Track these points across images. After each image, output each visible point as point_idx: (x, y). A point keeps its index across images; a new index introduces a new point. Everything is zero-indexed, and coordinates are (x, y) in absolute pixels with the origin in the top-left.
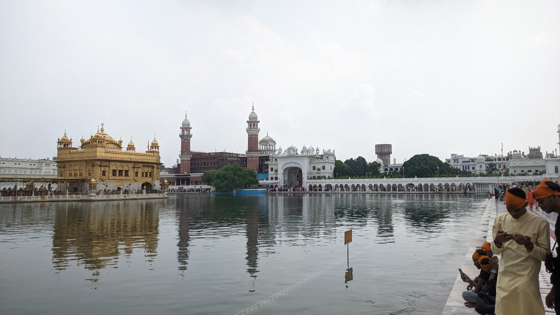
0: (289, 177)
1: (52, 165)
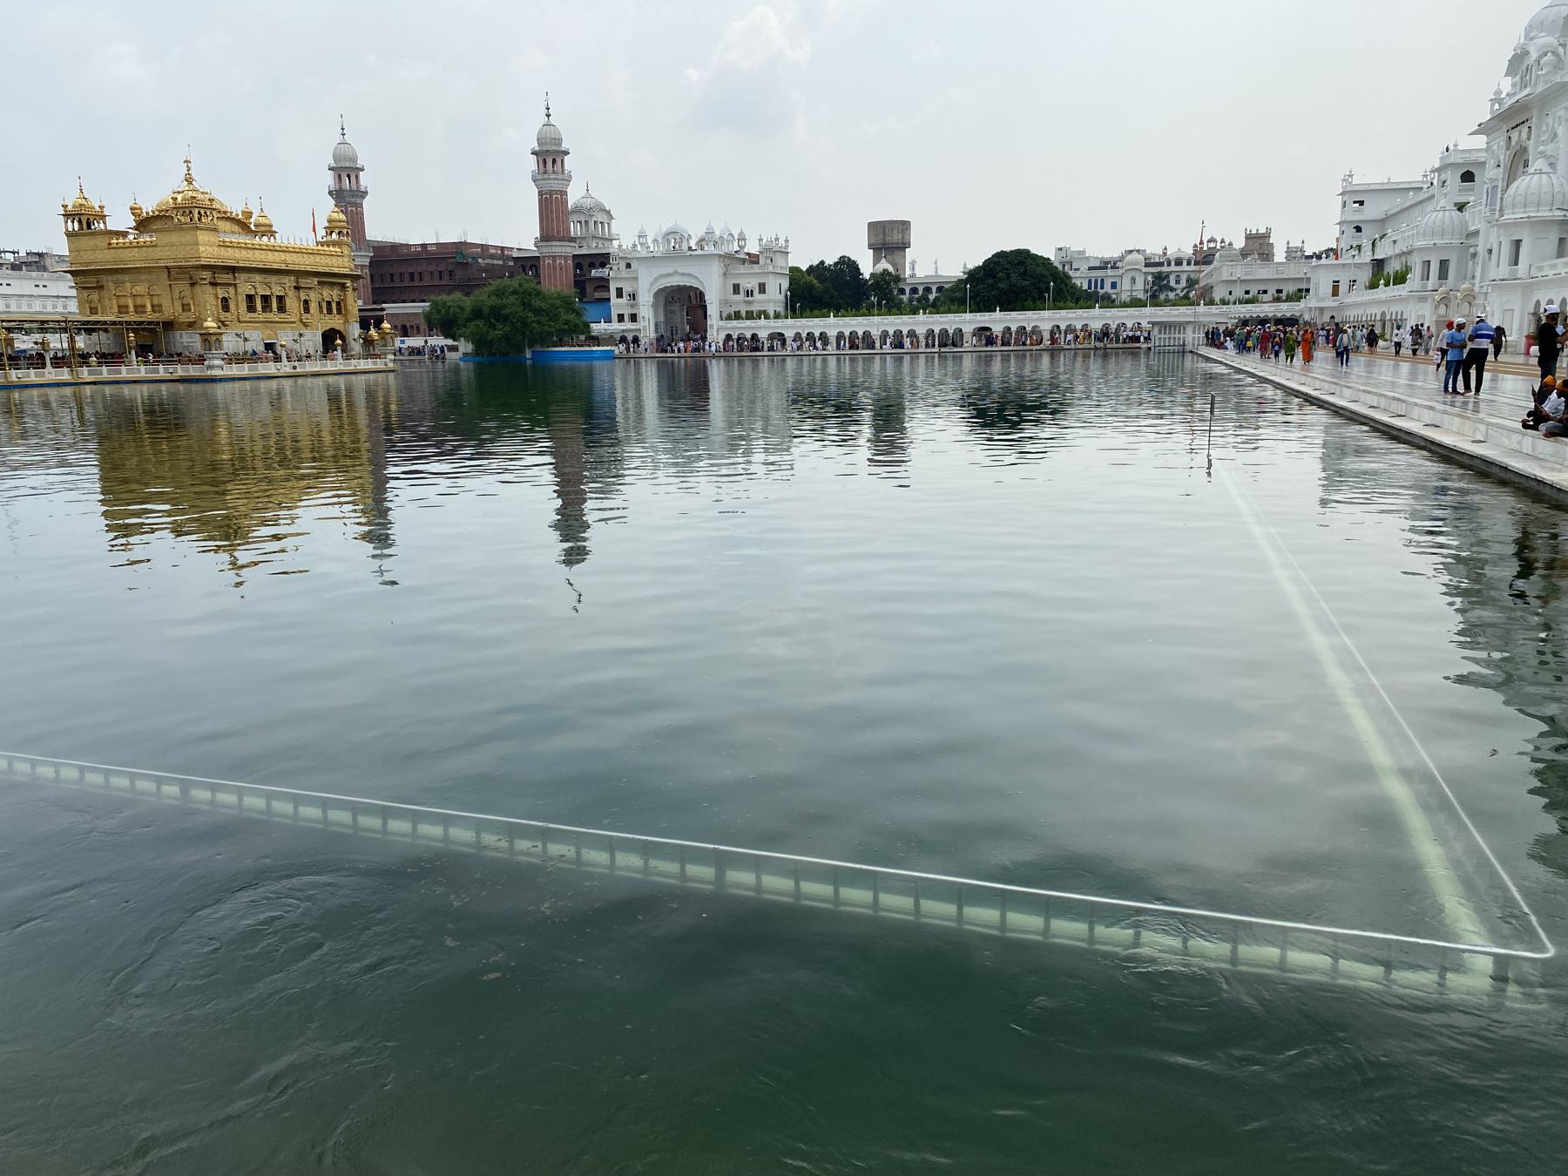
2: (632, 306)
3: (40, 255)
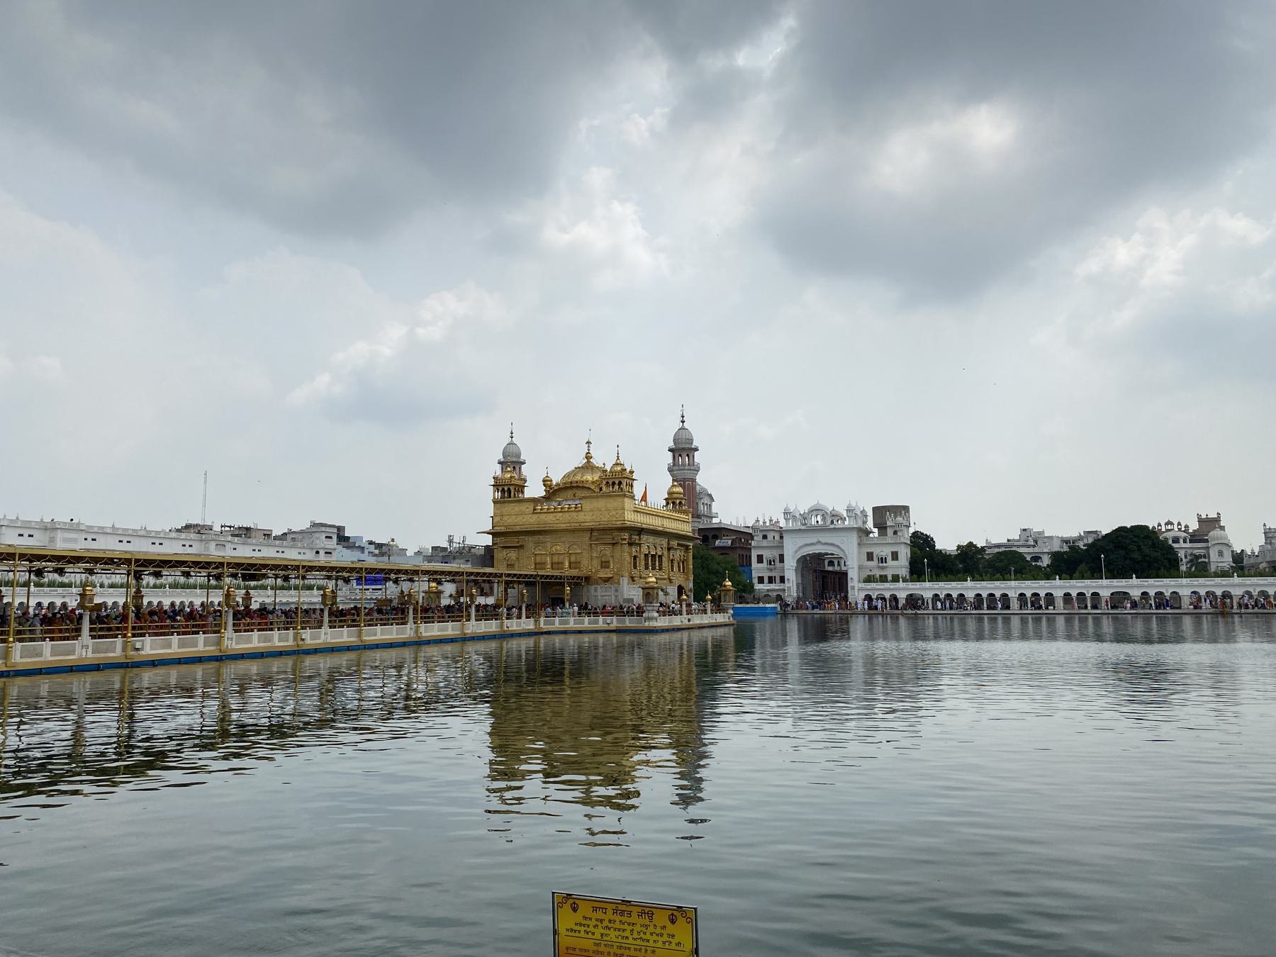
1: (229, 546)
3: (248, 529)
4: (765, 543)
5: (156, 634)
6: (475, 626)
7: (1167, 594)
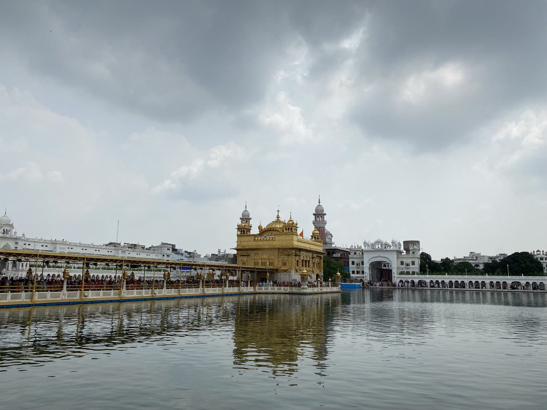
0: (372, 271)
1: (127, 252)
2: (358, 268)
3: (135, 245)
4: (355, 256)
5: (94, 290)
6: (228, 290)
7: (538, 283)
